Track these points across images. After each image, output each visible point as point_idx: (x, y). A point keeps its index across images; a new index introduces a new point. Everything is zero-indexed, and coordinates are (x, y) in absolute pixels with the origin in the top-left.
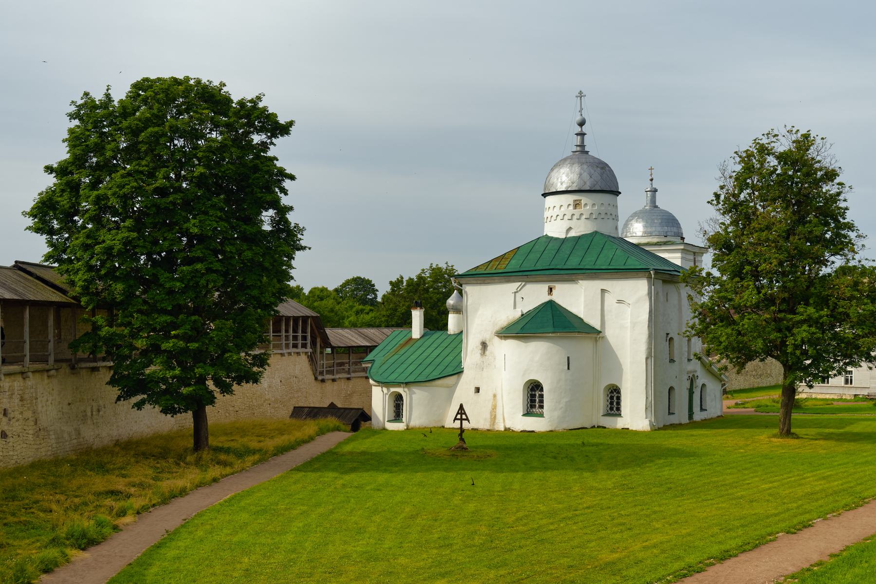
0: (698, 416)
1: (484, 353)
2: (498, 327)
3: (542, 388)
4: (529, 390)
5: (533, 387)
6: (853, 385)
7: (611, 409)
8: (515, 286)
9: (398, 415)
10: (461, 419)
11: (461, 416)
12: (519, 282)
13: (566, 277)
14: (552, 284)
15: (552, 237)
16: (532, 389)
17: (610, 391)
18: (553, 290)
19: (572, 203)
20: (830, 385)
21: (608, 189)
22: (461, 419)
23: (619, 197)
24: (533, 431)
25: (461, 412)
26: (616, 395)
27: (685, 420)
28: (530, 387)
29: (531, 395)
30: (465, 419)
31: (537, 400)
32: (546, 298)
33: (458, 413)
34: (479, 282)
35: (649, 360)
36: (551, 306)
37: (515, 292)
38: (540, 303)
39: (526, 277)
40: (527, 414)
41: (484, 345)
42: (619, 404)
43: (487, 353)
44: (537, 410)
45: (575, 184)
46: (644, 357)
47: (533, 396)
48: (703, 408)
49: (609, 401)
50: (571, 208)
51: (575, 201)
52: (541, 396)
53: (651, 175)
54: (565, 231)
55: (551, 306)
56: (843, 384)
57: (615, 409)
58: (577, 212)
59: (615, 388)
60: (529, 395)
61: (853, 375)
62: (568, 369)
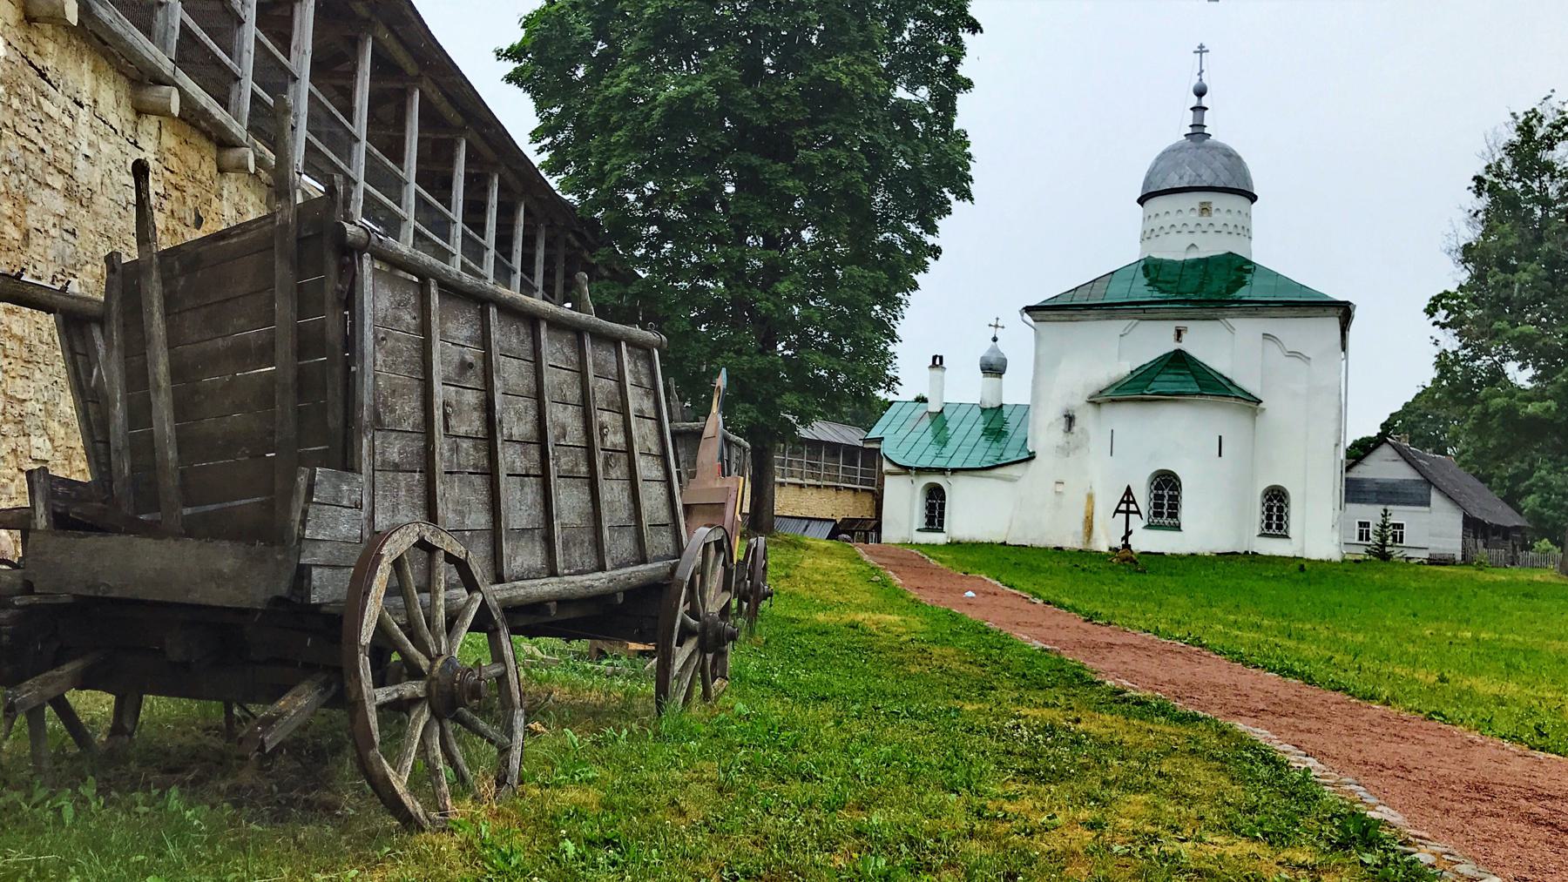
1: (1069, 430)
2: (1092, 390)
5: (1158, 483)
6: (1404, 544)
9: (935, 515)
10: (1128, 512)
11: (1128, 507)
19: (1197, 207)
22: (1128, 512)
24: (1162, 554)
25: (1128, 498)
28: (1155, 483)
30: (1133, 512)
32: (1170, 346)
33: (1122, 501)
36: (1178, 360)
38: (1161, 353)
41: (1070, 419)
44: (1165, 520)
50: (1195, 215)
51: (1202, 203)
55: (1178, 360)
58: (1205, 220)
60: (1152, 496)
61: (1405, 530)
62: (1220, 455)
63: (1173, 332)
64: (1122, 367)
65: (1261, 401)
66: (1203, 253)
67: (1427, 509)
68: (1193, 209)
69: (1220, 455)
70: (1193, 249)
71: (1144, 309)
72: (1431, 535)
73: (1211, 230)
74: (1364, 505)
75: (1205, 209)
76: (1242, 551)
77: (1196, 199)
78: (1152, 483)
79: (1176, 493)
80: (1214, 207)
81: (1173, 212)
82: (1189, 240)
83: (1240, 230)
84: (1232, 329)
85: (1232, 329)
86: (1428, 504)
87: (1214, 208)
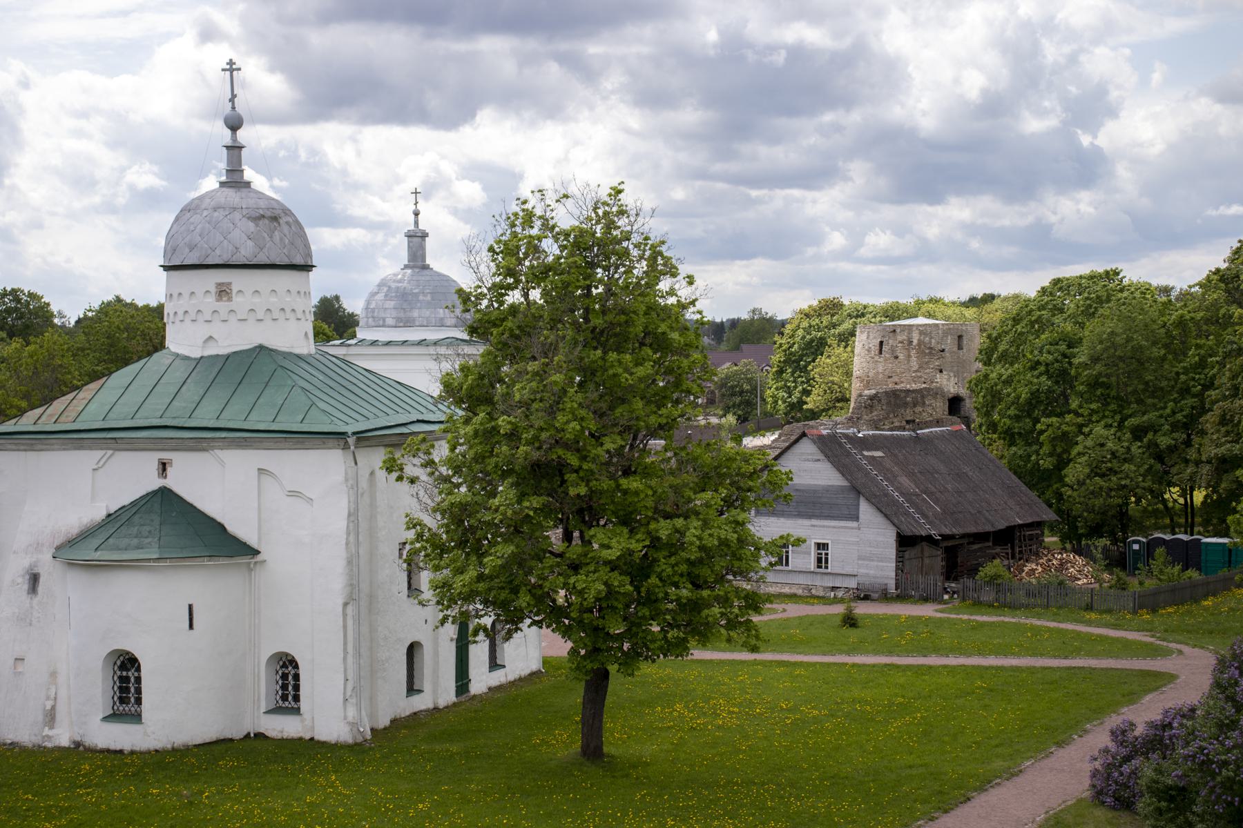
0: (481, 680)
3: (139, 666)
4: (116, 668)
5: (123, 663)
6: (829, 570)
7: (284, 698)
8: (99, 454)
12: (102, 449)
14: (165, 456)
15: (177, 355)
16: (123, 667)
17: (281, 663)
18: (169, 469)
19: (213, 289)
20: (790, 568)
21: (286, 261)
23: (312, 274)
26: (292, 672)
27: (447, 695)
28: (119, 663)
29: (120, 678)
31: (132, 690)
32: (155, 483)
34: (22, 447)
35: (350, 609)
37: (94, 470)
38: (143, 492)
39: (114, 441)
40: (114, 717)
42: (297, 688)
43: (40, 589)
46: (340, 601)
47: (126, 680)
48: (499, 662)
49: (280, 682)
50: (211, 299)
51: (219, 285)
52: (138, 680)
53: (416, 203)
54: (200, 342)
55: (165, 500)
56: (812, 566)
57: (290, 698)
58: (223, 306)
59: (289, 658)
60: (116, 678)
61: (829, 552)
62: (191, 626)
63: (154, 467)
64: (99, 513)
65: (258, 552)
66: (223, 348)
67: (855, 524)
68: (207, 291)
69: (191, 626)
70: (211, 343)
71: (115, 439)
72: (860, 558)
73: (233, 318)
74: (782, 520)
75: (223, 292)
76: (238, 734)
77: (211, 279)
78: (115, 663)
80: (235, 289)
81: (186, 295)
82: (203, 331)
83: (276, 314)
84: (222, 463)
85: (222, 463)
86: (856, 518)
87: (234, 292)
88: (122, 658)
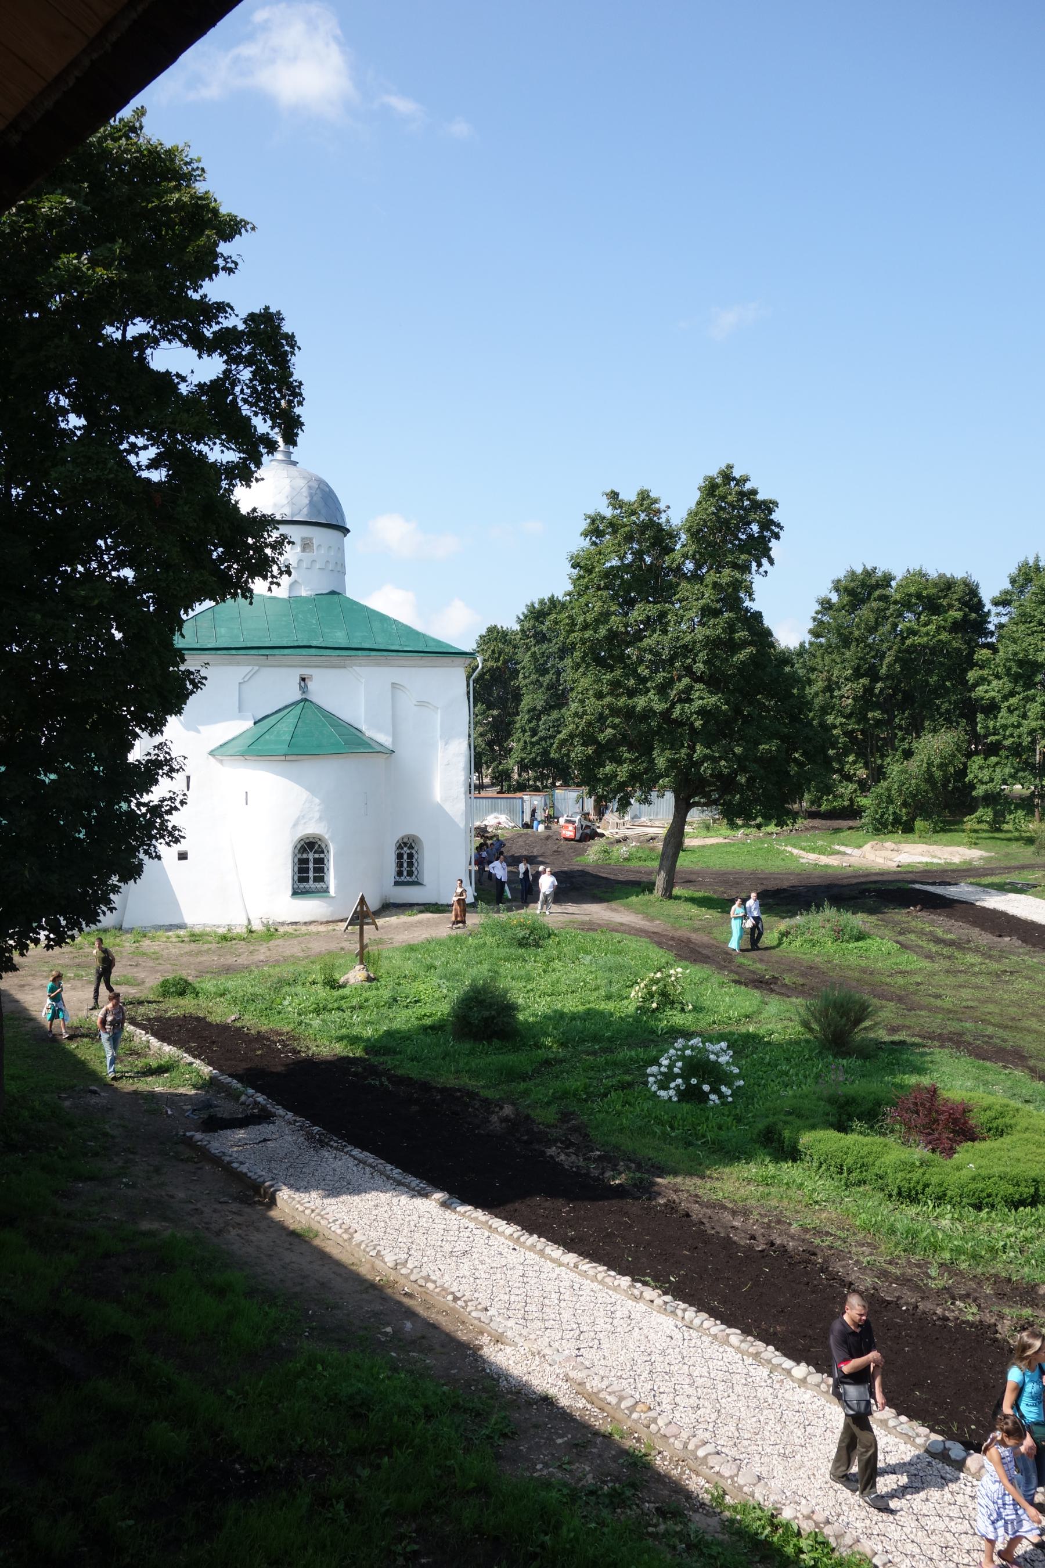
4: (297, 851)
13: (336, 660)
14: (305, 672)
28: (299, 846)
42: (410, 864)
44: (311, 884)
45: (305, 511)
47: (305, 861)
57: (405, 873)
63: (298, 679)
79: (322, 856)
88: (302, 843)
